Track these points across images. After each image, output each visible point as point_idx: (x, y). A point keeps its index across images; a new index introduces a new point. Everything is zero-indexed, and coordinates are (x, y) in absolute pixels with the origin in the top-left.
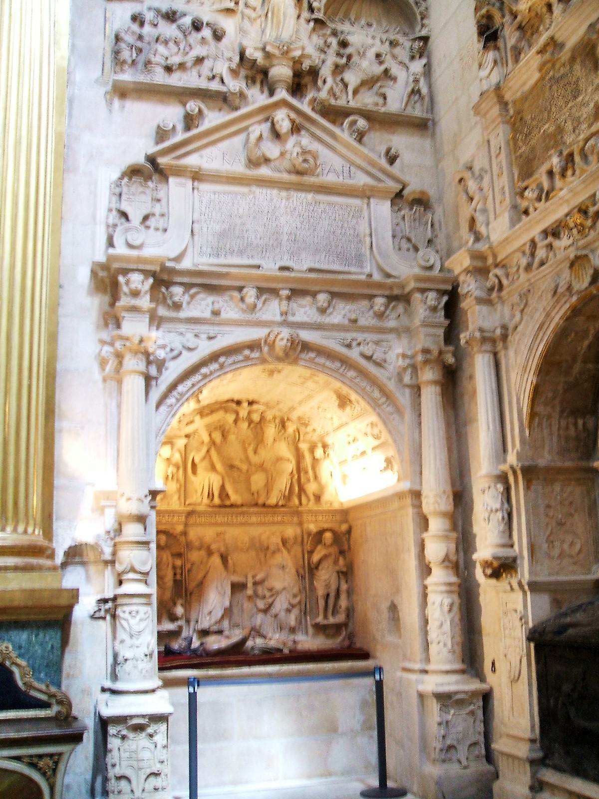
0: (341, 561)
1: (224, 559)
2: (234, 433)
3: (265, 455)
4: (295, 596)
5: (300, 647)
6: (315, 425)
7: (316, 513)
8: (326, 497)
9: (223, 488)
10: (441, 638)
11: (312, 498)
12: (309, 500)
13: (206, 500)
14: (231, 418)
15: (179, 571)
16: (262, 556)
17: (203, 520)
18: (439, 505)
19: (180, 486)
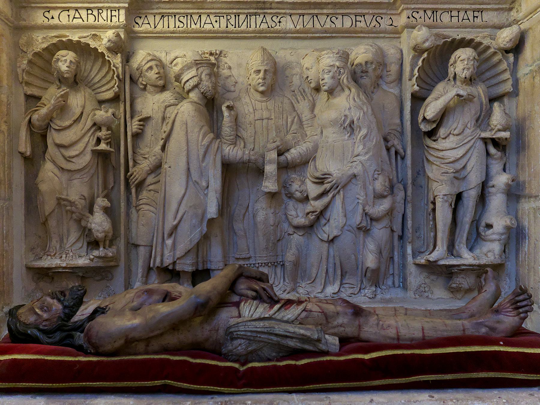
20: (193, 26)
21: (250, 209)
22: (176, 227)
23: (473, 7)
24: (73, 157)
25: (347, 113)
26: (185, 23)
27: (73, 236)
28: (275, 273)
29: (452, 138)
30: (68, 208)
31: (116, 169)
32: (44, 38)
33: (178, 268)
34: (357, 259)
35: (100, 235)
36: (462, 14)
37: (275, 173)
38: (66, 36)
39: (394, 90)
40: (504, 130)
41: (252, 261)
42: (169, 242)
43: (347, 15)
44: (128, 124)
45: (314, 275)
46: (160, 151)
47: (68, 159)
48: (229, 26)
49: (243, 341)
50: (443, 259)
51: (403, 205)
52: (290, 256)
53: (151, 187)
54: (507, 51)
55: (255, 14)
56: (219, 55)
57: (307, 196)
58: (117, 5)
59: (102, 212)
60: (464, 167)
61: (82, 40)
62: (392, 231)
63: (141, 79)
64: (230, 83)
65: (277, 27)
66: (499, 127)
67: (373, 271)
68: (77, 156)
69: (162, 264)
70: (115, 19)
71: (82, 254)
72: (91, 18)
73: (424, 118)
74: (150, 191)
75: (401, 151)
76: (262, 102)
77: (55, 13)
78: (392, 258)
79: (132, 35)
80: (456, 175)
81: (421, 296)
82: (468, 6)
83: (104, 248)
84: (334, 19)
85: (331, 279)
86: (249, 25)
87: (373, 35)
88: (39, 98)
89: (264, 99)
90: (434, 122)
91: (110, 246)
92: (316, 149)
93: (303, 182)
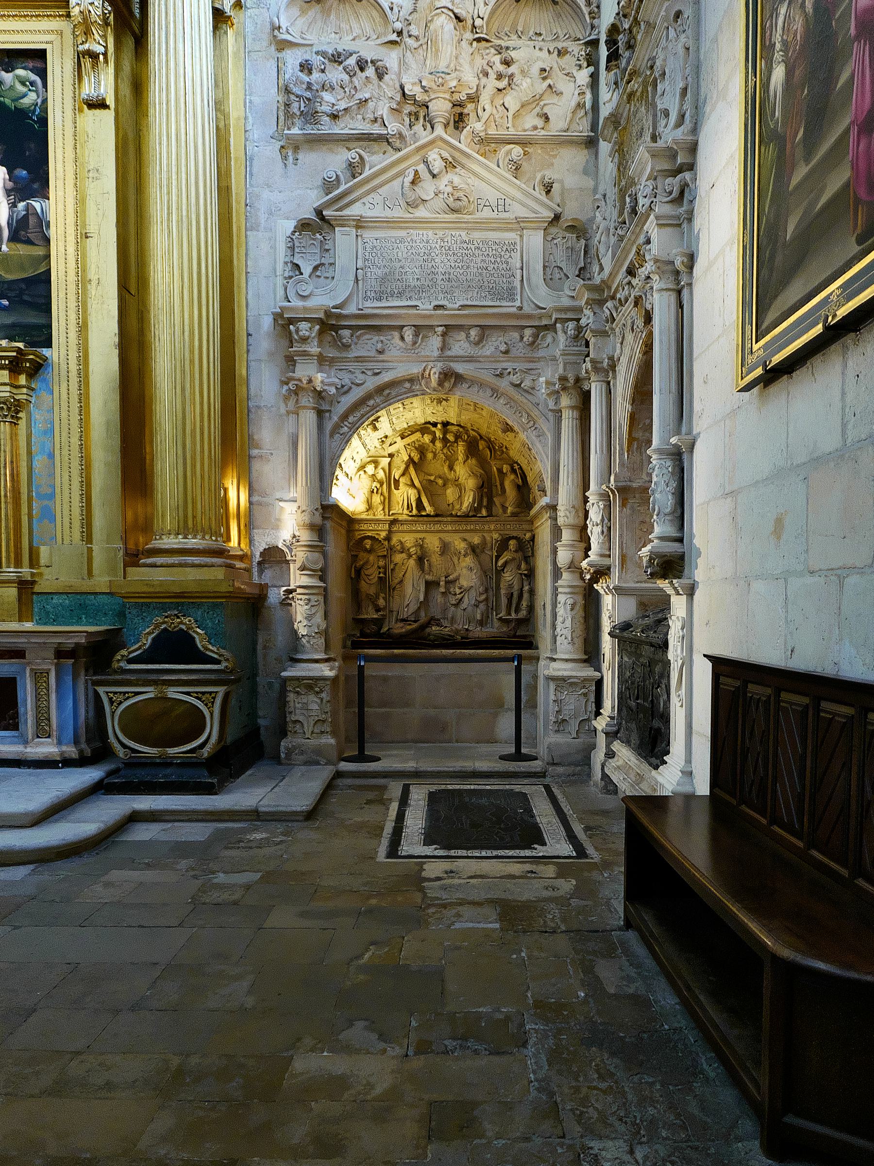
9: (419, 501)
13: (406, 512)
19: (384, 500)
56: (423, 539)
64: (427, 550)
88: (357, 556)
92: (459, 575)
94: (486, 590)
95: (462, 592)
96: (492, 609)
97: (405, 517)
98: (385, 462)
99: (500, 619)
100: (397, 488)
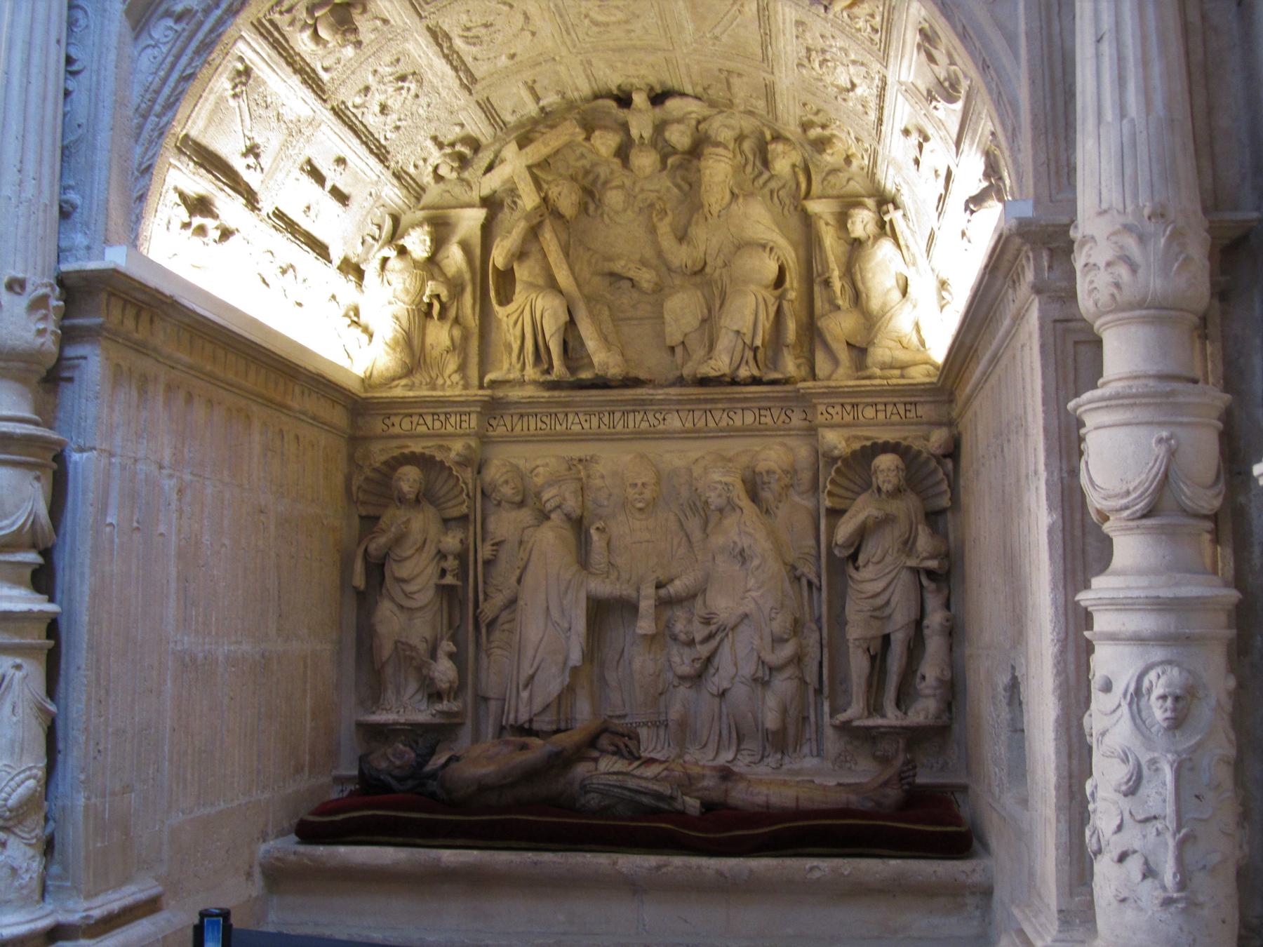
0: (924, 541)
1: (579, 525)
2: (622, 187)
3: (706, 240)
4: (778, 641)
5: (739, 795)
6: (845, 141)
7: (853, 399)
8: (882, 352)
10: (1133, 838)
11: (843, 355)
12: (836, 362)
13: (531, 373)
14: (605, 143)
15: (451, 563)
16: (693, 524)
17: (532, 427)
18: (1133, 268)
19: (465, 338)
20: (558, 427)
21: (626, 653)
22: (532, 677)
23: (902, 399)
24: (415, 593)
25: (736, 538)
26: (548, 423)
27: (413, 686)
28: (658, 736)
29: (871, 567)
30: (408, 653)
31: (463, 604)
32: (383, 450)
33: (536, 726)
34: (755, 719)
35: (445, 686)
36: (890, 408)
37: (652, 611)
38: (408, 447)
39: (808, 503)
40: (932, 557)
41: (628, 720)
42: (525, 695)
43: (748, 409)
44: (479, 549)
45: (705, 739)
46: (515, 584)
47: (408, 596)
48: (602, 425)
49: (596, 795)
50: (859, 719)
51: (819, 650)
52: (675, 713)
53: (506, 626)
54: (945, 456)
55: (634, 411)
57: (693, 639)
58: (468, 410)
59: (446, 658)
60: (888, 602)
61: (427, 452)
62: (806, 683)
63: (494, 495)
65: (661, 427)
66: (925, 554)
67: (775, 733)
68: (419, 591)
69: (516, 721)
70: (465, 425)
71: (422, 708)
72: (438, 424)
73: (836, 544)
74: (503, 631)
75: (815, 581)
76: (641, 520)
77: (396, 420)
78: (805, 719)
79: (485, 440)
80: (877, 614)
81: (840, 767)
82: (896, 400)
83: (449, 701)
84: (731, 414)
85: (726, 743)
86: (626, 426)
87: (782, 433)
89: (644, 516)
90: (852, 545)
91: (455, 699)
92: (707, 579)
93: (690, 621)
94: (797, 626)
95: (710, 637)
96: (819, 691)
97: (529, 391)
98: (470, 220)
99: (845, 729)
100: (505, 299)
